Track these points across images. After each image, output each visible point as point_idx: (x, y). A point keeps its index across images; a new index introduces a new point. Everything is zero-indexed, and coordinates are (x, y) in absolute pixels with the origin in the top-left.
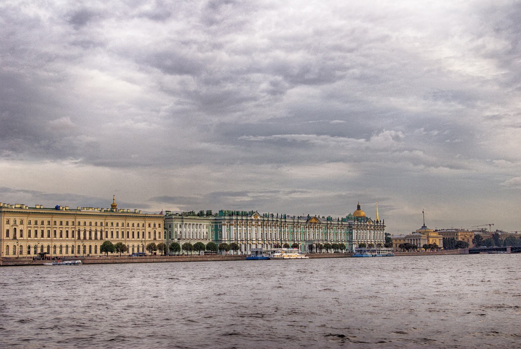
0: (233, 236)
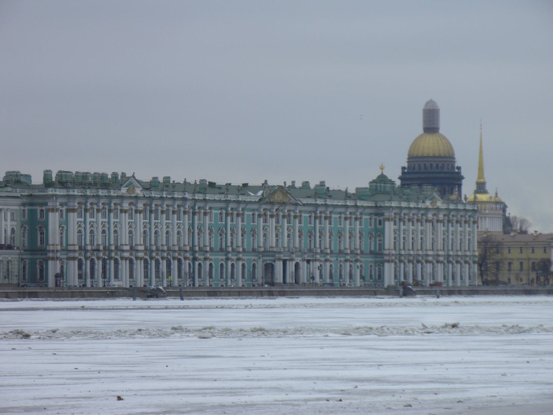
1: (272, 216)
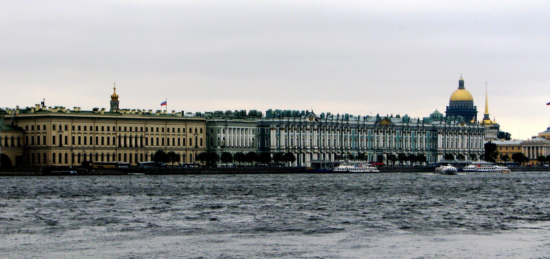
0: (283, 143)
1: (381, 132)
